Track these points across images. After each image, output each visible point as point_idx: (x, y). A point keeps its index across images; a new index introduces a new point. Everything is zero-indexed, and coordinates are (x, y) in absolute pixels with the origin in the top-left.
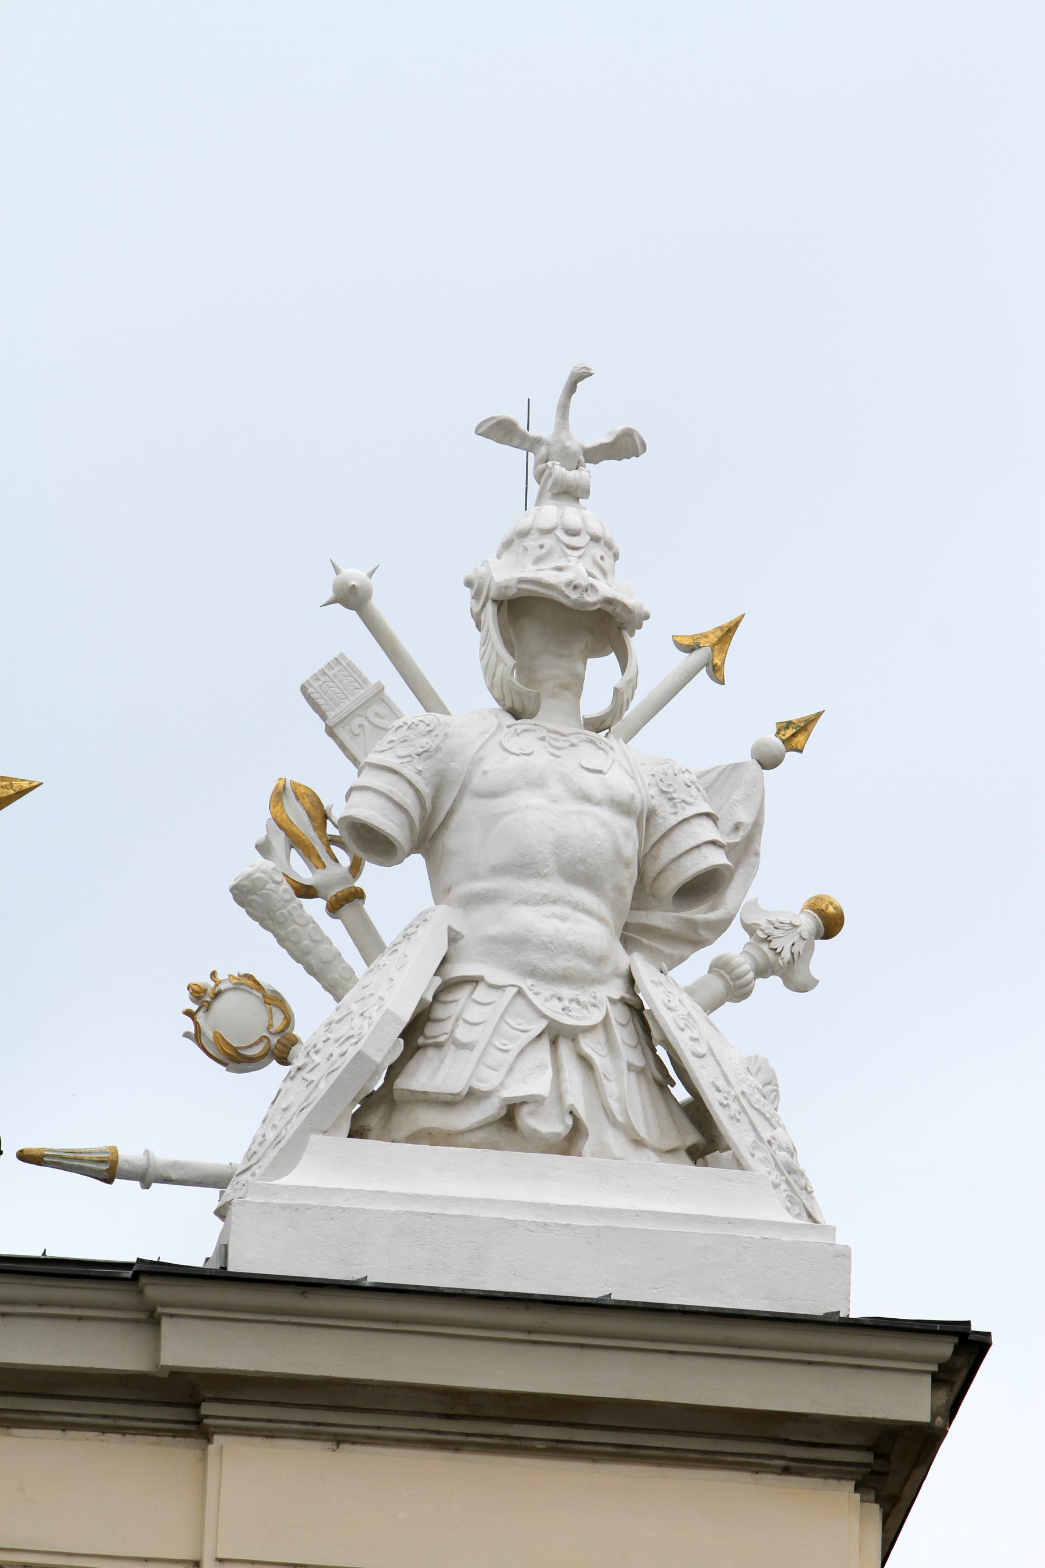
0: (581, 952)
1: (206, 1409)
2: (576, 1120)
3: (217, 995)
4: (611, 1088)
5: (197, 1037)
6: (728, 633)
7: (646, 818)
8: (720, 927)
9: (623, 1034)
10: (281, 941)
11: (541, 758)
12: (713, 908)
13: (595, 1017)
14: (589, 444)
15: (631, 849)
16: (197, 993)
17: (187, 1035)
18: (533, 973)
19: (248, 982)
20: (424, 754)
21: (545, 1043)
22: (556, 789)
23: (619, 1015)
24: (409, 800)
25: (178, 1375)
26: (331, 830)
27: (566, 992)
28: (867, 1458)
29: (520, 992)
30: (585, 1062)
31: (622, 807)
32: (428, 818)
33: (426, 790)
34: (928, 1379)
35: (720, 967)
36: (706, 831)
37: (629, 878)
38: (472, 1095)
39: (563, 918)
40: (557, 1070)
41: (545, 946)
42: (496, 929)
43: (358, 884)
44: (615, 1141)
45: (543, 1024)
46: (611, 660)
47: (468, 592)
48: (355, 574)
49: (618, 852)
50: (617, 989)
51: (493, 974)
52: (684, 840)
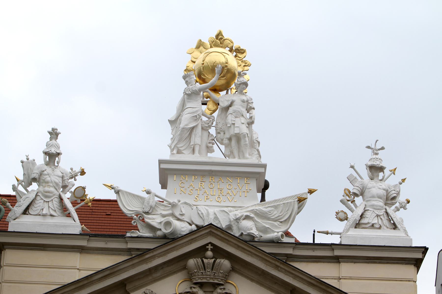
0: (380, 206)
1: (340, 260)
2: (380, 225)
3: (339, 213)
4: (384, 222)
5: (337, 218)
6: (395, 169)
7: (387, 191)
8: (396, 203)
9: (385, 215)
10: (346, 206)
11: (375, 184)
12: (395, 201)
13: (382, 214)
14: (378, 148)
15: (385, 194)
16: (337, 213)
17: (336, 217)
18: (375, 209)
19: (342, 211)
21: (376, 217)
22: (376, 188)
23: (385, 213)
24: (360, 190)
25: (336, 256)
26: (351, 194)
27: (379, 211)
28: (415, 262)
29: (373, 211)
30: (381, 219)
31: (384, 190)
32: (362, 192)
33: (362, 188)
34: (422, 253)
35: (396, 207)
36: (394, 192)
37: (385, 197)
38: (368, 223)
39: (378, 202)
41: (376, 206)
42: (370, 204)
43: (354, 200)
44: (385, 228)
45: (376, 215)
47: (365, 166)
48: (352, 164)
49: (384, 195)
50: (384, 210)
51: (370, 209)
52: (391, 193)
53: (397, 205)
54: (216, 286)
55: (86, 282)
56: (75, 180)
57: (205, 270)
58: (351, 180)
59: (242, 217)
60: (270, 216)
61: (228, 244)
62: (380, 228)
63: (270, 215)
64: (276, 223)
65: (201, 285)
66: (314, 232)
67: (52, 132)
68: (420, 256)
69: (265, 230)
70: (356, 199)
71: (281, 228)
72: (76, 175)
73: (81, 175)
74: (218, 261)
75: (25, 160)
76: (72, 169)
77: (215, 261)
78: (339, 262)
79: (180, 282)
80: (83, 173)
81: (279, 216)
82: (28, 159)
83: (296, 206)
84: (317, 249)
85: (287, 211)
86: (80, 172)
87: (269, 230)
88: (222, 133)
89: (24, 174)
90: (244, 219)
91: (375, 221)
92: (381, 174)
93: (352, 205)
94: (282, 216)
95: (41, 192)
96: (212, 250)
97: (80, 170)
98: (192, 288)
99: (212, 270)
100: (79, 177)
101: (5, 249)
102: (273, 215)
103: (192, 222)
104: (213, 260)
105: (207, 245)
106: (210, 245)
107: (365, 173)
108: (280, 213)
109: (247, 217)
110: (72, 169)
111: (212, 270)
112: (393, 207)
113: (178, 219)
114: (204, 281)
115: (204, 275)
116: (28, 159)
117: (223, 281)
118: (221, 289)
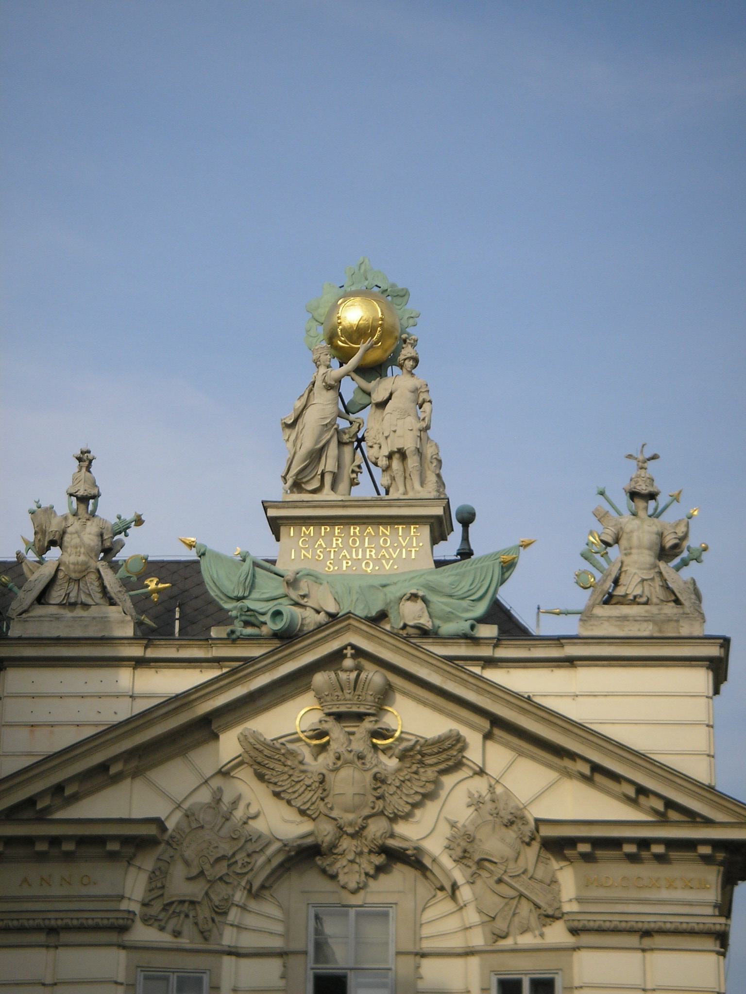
6: (680, 493)
8: (682, 552)
14: (647, 457)
20: (616, 525)
40: (643, 588)
46: (653, 501)
47: (624, 491)
48: (601, 487)
52: (668, 538)
53: (685, 554)
54: (364, 717)
55: (141, 721)
56: (126, 535)
57: (343, 691)
58: (601, 517)
59: (405, 596)
60: (453, 591)
61: (380, 644)
62: (646, 603)
63: (453, 588)
64: (465, 603)
65: (339, 717)
66: (539, 608)
67: (82, 456)
68: (714, 651)
69: (448, 617)
70: (609, 549)
71: (472, 610)
72: (129, 528)
73: (135, 525)
74: (363, 675)
75: (35, 508)
76: (119, 518)
77: (358, 676)
78: (575, 667)
79: (303, 712)
80: (139, 521)
81: (469, 591)
82: (39, 507)
83: (497, 571)
84: (535, 646)
85: (483, 580)
86: (135, 521)
87: (452, 616)
88: (376, 447)
89: (36, 533)
90: (408, 600)
91: (638, 591)
92: (652, 503)
93: (602, 561)
94: (476, 589)
95: (65, 563)
96: (353, 656)
97: (135, 518)
98: (323, 722)
99: (355, 690)
100: (133, 530)
101: (5, 668)
102: (457, 589)
103: (322, 608)
104: (355, 674)
105: (345, 648)
106: (349, 648)
107: (623, 501)
108: (471, 585)
109: (414, 597)
110: (119, 518)
111: (355, 690)
112: (677, 560)
113: (296, 604)
114: (343, 709)
115: (340, 700)
116: (39, 507)
117: (374, 708)
118: (371, 722)
